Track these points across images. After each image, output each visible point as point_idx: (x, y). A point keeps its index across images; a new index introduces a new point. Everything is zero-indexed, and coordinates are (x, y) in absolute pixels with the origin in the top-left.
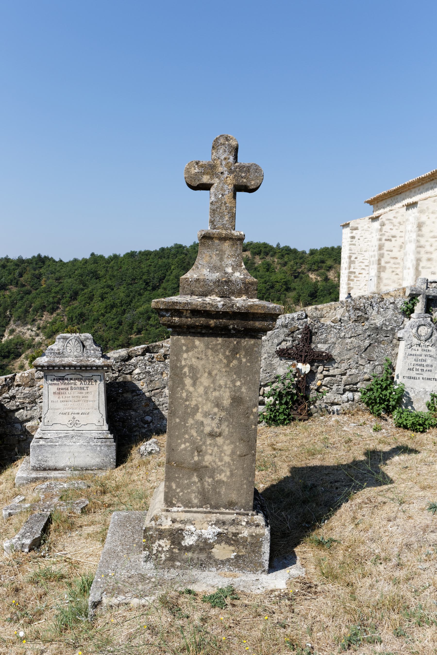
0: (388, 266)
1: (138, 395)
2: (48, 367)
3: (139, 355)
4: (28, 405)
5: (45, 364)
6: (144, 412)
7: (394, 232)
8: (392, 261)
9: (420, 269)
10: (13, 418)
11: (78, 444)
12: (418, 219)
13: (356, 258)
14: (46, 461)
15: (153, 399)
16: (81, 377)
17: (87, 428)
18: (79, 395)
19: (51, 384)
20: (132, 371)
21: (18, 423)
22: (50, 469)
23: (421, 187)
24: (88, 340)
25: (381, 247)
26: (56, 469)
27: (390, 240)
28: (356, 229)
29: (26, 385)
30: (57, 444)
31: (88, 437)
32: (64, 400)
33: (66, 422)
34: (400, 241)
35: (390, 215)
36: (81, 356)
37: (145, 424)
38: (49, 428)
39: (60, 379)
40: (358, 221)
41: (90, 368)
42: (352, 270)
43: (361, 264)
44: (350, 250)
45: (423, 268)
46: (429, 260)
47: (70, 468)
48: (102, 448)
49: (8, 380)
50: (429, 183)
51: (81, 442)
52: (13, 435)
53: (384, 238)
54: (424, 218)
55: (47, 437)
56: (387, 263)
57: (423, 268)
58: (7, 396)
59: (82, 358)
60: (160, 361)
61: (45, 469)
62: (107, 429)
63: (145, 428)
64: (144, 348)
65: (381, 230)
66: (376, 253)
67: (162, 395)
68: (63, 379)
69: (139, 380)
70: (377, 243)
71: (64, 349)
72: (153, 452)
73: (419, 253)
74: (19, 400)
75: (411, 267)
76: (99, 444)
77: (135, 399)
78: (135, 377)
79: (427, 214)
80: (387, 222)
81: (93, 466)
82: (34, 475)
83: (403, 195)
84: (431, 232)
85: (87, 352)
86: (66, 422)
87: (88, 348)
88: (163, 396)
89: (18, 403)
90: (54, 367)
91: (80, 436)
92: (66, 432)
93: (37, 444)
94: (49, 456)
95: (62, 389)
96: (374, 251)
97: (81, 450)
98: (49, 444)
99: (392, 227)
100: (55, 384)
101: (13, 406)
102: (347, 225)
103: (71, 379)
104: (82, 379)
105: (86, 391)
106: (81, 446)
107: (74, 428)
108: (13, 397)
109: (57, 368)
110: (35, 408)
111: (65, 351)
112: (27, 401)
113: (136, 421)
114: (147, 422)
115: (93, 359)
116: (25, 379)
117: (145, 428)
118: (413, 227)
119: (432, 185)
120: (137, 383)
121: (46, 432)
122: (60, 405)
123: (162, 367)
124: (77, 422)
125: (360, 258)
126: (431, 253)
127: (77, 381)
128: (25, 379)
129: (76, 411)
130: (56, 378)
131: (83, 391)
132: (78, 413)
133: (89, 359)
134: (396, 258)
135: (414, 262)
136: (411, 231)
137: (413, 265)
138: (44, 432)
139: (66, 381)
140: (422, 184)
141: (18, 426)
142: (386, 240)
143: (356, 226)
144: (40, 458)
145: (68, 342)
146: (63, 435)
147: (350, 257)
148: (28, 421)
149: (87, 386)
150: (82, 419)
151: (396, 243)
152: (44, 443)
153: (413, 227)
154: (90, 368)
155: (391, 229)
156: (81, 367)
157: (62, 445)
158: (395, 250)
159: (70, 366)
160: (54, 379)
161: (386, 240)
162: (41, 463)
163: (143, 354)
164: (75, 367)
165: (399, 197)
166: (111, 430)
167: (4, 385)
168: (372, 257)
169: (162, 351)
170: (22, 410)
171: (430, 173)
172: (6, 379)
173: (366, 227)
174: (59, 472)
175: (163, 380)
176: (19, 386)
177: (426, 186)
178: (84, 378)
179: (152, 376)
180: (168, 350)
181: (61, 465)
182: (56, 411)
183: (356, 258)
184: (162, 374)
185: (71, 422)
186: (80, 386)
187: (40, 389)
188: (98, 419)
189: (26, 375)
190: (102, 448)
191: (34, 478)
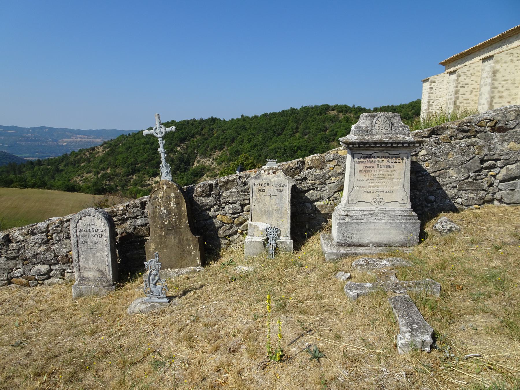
0: (461, 105)
1: (423, 176)
2: (359, 144)
3: (425, 137)
4: (318, 186)
5: (357, 141)
6: (428, 192)
7: (467, 81)
8: (465, 102)
9: (493, 104)
10: (304, 198)
11: (383, 221)
12: (493, 68)
13: (433, 102)
14: (351, 238)
15: (437, 179)
16: (388, 155)
17: (390, 205)
18: (385, 173)
19: (358, 163)
20: (418, 153)
21: (308, 202)
22: (354, 246)
23: (490, 47)
24: (395, 117)
25: (457, 92)
26: (360, 246)
27: (464, 87)
28: (434, 82)
29: (317, 167)
30: (363, 221)
31: (393, 215)
32: (369, 178)
33: (370, 200)
34: (471, 87)
35: (465, 69)
36: (389, 134)
37: (428, 203)
38: (354, 206)
39: (367, 157)
40: (435, 76)
41: (401, 145)
42: (430, 111)
43: (436, 106)
44: (429, 97)
45: (496, 103)
46: (500, 97)
47: (373, 244)
48: (407, 225)
49: (299, 163)
50: (497, 44)
51: (386, 219)
52: (303, 214)
53: (459, 85)
54: (498, 67)
55: (352, 215)
56: (461, 103)
57: (496, 103)
58: (299, 177)
59: (390, 136)
60: (446, 142)
61: (349, 246)
62: (410, 207)
63: (428, 207)
64: (430, 130)
65: (457, 80)
66: (453, 97)
67: (446, 175)
68: (370, 158)
69: (424, 161)
70: (454, 90)
71: (372, 127)
72: (454, 229)
73: (493, 92)
74: (310, 182)
75: (486, 103)
76: (404, 221)
77: (420, 180)
78: (421, 158)
79: (500, 64)
80: (462, 74)
81: (396, 243)
82: (342, 251)
83: (472, 55)
84: (503, 76)
85: (396, 129)
86: (370, 200)
87: (396, 125)
88: (447, 176)
89: (309, 185)
90: (365, 144)
91: (385, 214)
92: (369, 209)
93: (343, 221)
94: (355, 232)
95: (369, 167)
96: (451, 95)
97: (386, 227)
98: (355, 221)
99: (465, 78)
100: (362, 162)
101: (305, 187)
102: (427, 80)
103: (378, 157)
104: (389, 157)
105: (392, 169)
106: (386, 223)
107: (378, 206)
108: (305, 179)
109: (368, 145)
110: (324, 189)
111: (373, 128)
112: (318, 182)
113: (420, 200)
114: (431, 202)
115: (402, 136)
116: (316, 162)
117: (428, 207)
118: (489, 74)
119: (500, 44)
120: (422, 164)
121: (350, 209)
122: (364, 183)
123: (448, 148)
124: (381, 200)
125: (436, 102)
126: (502, 92)
127: (383, 159)
128: (316, 162)
129: (381, 189)
130: (363, 156)
131: (389, 169)
132: (383, 192)
133: (398, 136)
134: (468, 99)
135: (489, 100)
136: (487, 77)
137: (488, 102)
138: (348, 210)
139: (373, 159)
140: (492, 44)
141: (308, 205)
142: (461, 87)
143: (434, 80)
144: (345, 234)
145: (377, 120)
146: (368, 213)
147: (429, 102)
148: (317, 200)
149: (393, 164)
150: (386, 197)
151: (468, 89)
152: (350, 220)
153: (489, 74)
154: (401, 145)
155: (465, 79)
156: (392, 143)
157: (367, 222)
158: (467, 94)
159: (381, 143)
160: (361, 157)
161: (461, 87)
162: (346, 240)
163: (429, 136)
164: (386, 143)
165: (468, 57)
166: (414, 208)
167: (297, 167)
168: (449, 100)
169: (449, 132)
170: (312, 191)
171: (501, 34)
172: (298, 162)
173: (441, 81)
174: (364, 248)
175: (449, 161)
176: (310, 168)
177: (494, 46)
178: (391, 156)
179: (438, 157)
180: (455, 132)
181: (366, 241)
182: (361, 189)
183: (433, 102)
184: (448, 155)
185: (375, 200)
186: (386, 164)
187: (330, 171)
188: (402, 197)
189: (317, 158)
190: (407, 225)
191: (344, 254)
